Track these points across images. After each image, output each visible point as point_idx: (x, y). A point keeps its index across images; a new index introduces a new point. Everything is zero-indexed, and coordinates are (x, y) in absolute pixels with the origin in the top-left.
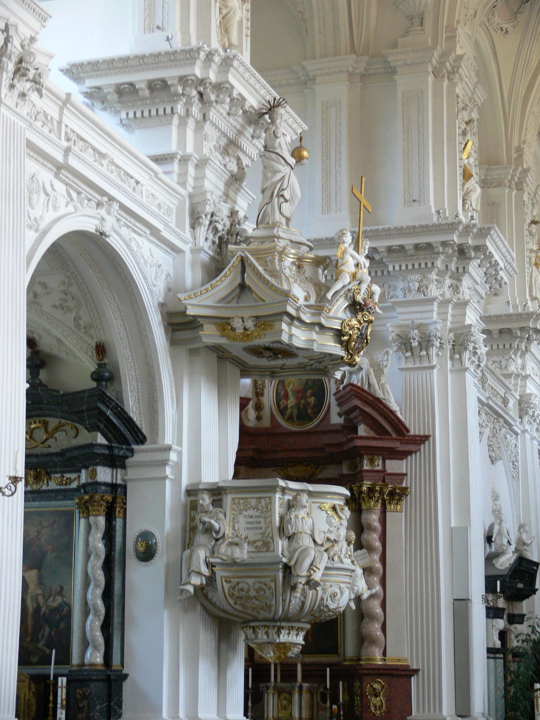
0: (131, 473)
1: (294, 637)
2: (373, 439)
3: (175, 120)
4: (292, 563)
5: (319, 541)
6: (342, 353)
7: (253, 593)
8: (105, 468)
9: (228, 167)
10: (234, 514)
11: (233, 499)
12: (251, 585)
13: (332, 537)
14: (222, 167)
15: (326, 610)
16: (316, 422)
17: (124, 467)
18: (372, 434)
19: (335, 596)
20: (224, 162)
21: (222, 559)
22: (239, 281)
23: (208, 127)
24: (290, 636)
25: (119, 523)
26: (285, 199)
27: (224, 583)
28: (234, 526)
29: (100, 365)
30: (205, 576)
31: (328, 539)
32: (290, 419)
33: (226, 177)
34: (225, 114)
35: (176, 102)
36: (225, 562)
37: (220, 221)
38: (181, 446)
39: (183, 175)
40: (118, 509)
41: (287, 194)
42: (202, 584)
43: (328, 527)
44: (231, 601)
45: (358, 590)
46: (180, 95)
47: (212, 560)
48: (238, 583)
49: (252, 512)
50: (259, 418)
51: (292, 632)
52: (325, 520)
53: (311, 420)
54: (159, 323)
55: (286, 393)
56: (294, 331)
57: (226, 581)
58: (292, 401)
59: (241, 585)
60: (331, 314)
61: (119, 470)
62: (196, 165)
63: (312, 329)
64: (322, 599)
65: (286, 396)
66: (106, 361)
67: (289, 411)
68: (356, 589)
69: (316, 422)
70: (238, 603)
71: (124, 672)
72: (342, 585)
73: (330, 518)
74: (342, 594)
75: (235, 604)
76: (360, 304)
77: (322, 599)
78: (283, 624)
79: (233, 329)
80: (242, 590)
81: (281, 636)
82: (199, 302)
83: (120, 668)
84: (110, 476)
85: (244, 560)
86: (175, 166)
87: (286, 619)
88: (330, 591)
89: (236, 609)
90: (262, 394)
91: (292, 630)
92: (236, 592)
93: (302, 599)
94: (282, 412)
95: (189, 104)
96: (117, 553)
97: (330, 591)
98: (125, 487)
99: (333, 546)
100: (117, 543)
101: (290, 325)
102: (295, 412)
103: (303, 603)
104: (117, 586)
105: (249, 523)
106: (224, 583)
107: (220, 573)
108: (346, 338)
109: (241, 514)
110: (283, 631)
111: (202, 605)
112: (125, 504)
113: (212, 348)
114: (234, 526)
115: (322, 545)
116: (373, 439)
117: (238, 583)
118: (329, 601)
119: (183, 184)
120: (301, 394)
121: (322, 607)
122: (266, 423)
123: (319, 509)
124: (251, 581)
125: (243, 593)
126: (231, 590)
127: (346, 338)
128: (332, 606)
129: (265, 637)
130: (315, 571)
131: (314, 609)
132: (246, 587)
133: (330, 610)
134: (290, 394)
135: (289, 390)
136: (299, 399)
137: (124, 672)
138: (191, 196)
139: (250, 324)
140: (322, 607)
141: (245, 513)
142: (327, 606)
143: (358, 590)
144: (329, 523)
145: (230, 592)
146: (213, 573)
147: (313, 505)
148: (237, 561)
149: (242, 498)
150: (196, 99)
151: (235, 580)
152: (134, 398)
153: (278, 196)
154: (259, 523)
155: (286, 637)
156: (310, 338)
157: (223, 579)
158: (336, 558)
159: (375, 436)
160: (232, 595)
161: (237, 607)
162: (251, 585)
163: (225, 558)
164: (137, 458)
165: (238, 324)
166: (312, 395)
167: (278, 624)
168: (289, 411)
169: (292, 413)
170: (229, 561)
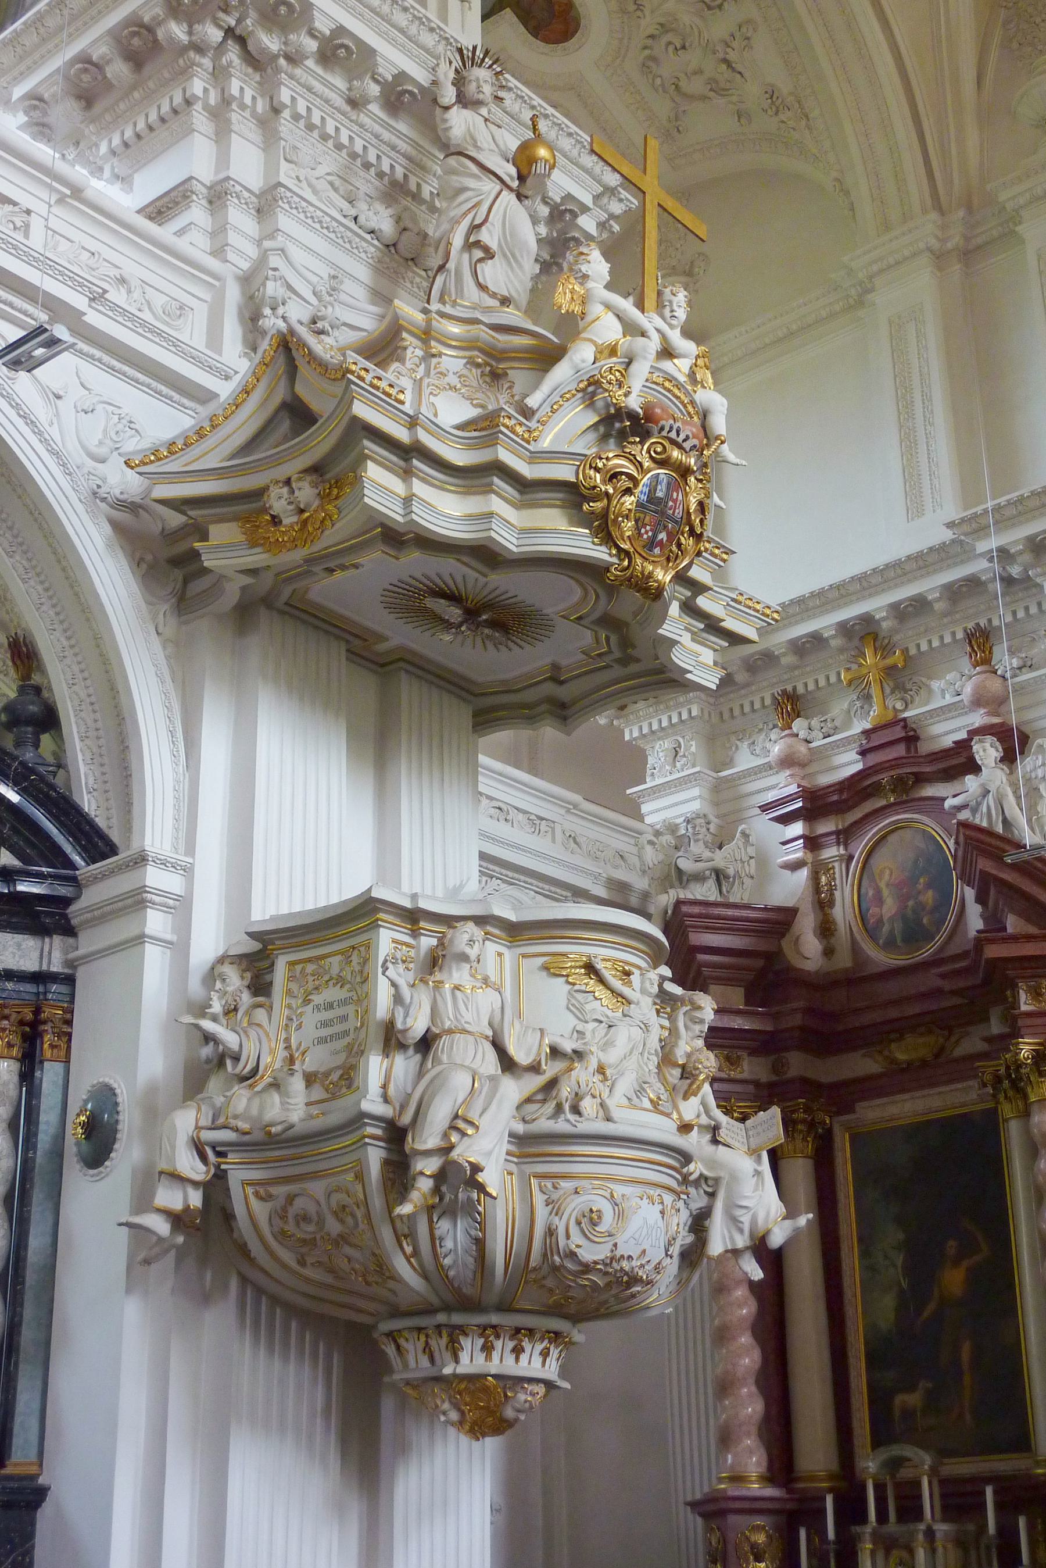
0: (88, 942)
1: (510, 1359)
2: (1029, 938)
3: (199, 119)
4: (406, 1119)
5: (521, 1056)
6: (601, 553)
7: (334, 1227)
8: (19, 937)
9: (362, 219)
10: (289, 1007)
11: (292, 964)
12: (323, 1201)
13: (568, 1046)
14: (352, 225)
15: (570, 1265)
16: (939, 939)
17: (69, 931)
18: (1032, 930)
19: (594, 1224)
20: (353, 212)
21: (236, 1130)
22: (280, 395)
23: (285, 124)
24: (496, 1355)
25: (50, 1074)
26: (486, 249)
27: (252, 1199)
28: (287, 1040)
29: (22, 690)
30: (195, 1184)
31: (555, 1052)
32: (890, 945)
33: (372, 248)
34: (339, 102)
35: (185, 73)
36: (246, 1138)
37: (328, 327)
38: (193, 856)
39: (219, 233)
40: (47, 1038)
41: (488, 237)
42: (187, 1209)
43: (572, 1021)
44: (287, 1257)
45: (754, 1221)
46: (184, 50)
47: (207, 1136)
48: (290, 1199)
49: (333, 994)
50: (828, 952)
51: (498, 1344)
52: (564, 1002)
53: (930, 937)
54: (108, 546)
55: (878, 892)
56: (419, 488)
57: (256, 1194)
58: (889, 907)
59: (299, 1203)
60: (546, 443)
61: (57, 939)
62: (258, 211)
63: (488, 490)
64: (551, 1232)
65: (879, 900)
66: (36, 679)
67: (886, 929)
68: (746, 1219)
69: (939, 939)
70: (310, 1260)
71: (41, 1480)
72: (619, 1190)
73: (579, 996)
74: (620, 1215)
75: (302, 1263)
76: (632, 416)
77: (551, 1232)
78: (457, 1319)
79: (276, 521)
80: (304, 1218)
81: (464, 1357)
82: (186, 465)
83: (33, 1470)
84: (36, 955)
85: (292, 1126)
86: (197, 214)
87: (469, 1305)
88: (574, 1206)
89: (308, 1280)
90: (831, 903)
91: (498, 1337)
92: (291, 1227)
93: (473, 1233)
94: (872, 933)
95: (219, 75)
96: (39, 1153)
97: (574, 1206)
98: (70, 980)
99: (570, 1069)
100: (42, 1127)
101: (407, 474)
102: (898, 926)
103: (480, 1243)
104: (36, 1242)
105: (325, 1024)
106: (253, 1201)
107: (237, 1176)
108: (598, 506)
109: (307, 1002)
110: (466, 1343)
111: (244, 1280)
112: (69, 1023)
113: (287, 609)
114: (287, 1040)
115: (535, 1068)
116: (1029, 938)
117: (290, 1199)
118: (576, 1238)
119: (219, 252)
120: (905, 889)
121: (557, 1258)
122: (844, 960)
123: (544, 973)
124: (317, 1188)
125: (311, 1228)
126: (277, 1221)
127: (598, 506)
128: (589, 1253)
129: (425, 1362)
130: (464, 1134)
131: (533, 1263)
132: (312, 1209)
133: (587, 1268)
134: (885, 892)
135: (882, 885)
136: (903, 899)
137: (41, 1480)
138: (246, 280)
139: (306, 492)
140: (557, 1258)
141: (317, 999)
142: (572, 1255)
143: (754, 1221)
144: (576, 1010)
145: (276, 1229)
146: (220, 1176)
147: (525, 963)
148: (273, 1130)
149: (309, 960)
150: (233, 55)
151: (280, 1191)
152: (89, 756)
153: (470, 245)
154: (344, 1018)
155: (480, 1358)
156: (486, 510)
157: (249, 1190)
158: (588, 1105)
159: (1032, 930)
160: (282, 1236)
161: (308, 1272)
162: (323, 1201)
163: (244, 1126)
164: (90, 897)
165: (278, 502)
166: (929, 886)
167: (441, 1318)
168: (886, 929)
169: (892, 931)
170: (258, 1136)
